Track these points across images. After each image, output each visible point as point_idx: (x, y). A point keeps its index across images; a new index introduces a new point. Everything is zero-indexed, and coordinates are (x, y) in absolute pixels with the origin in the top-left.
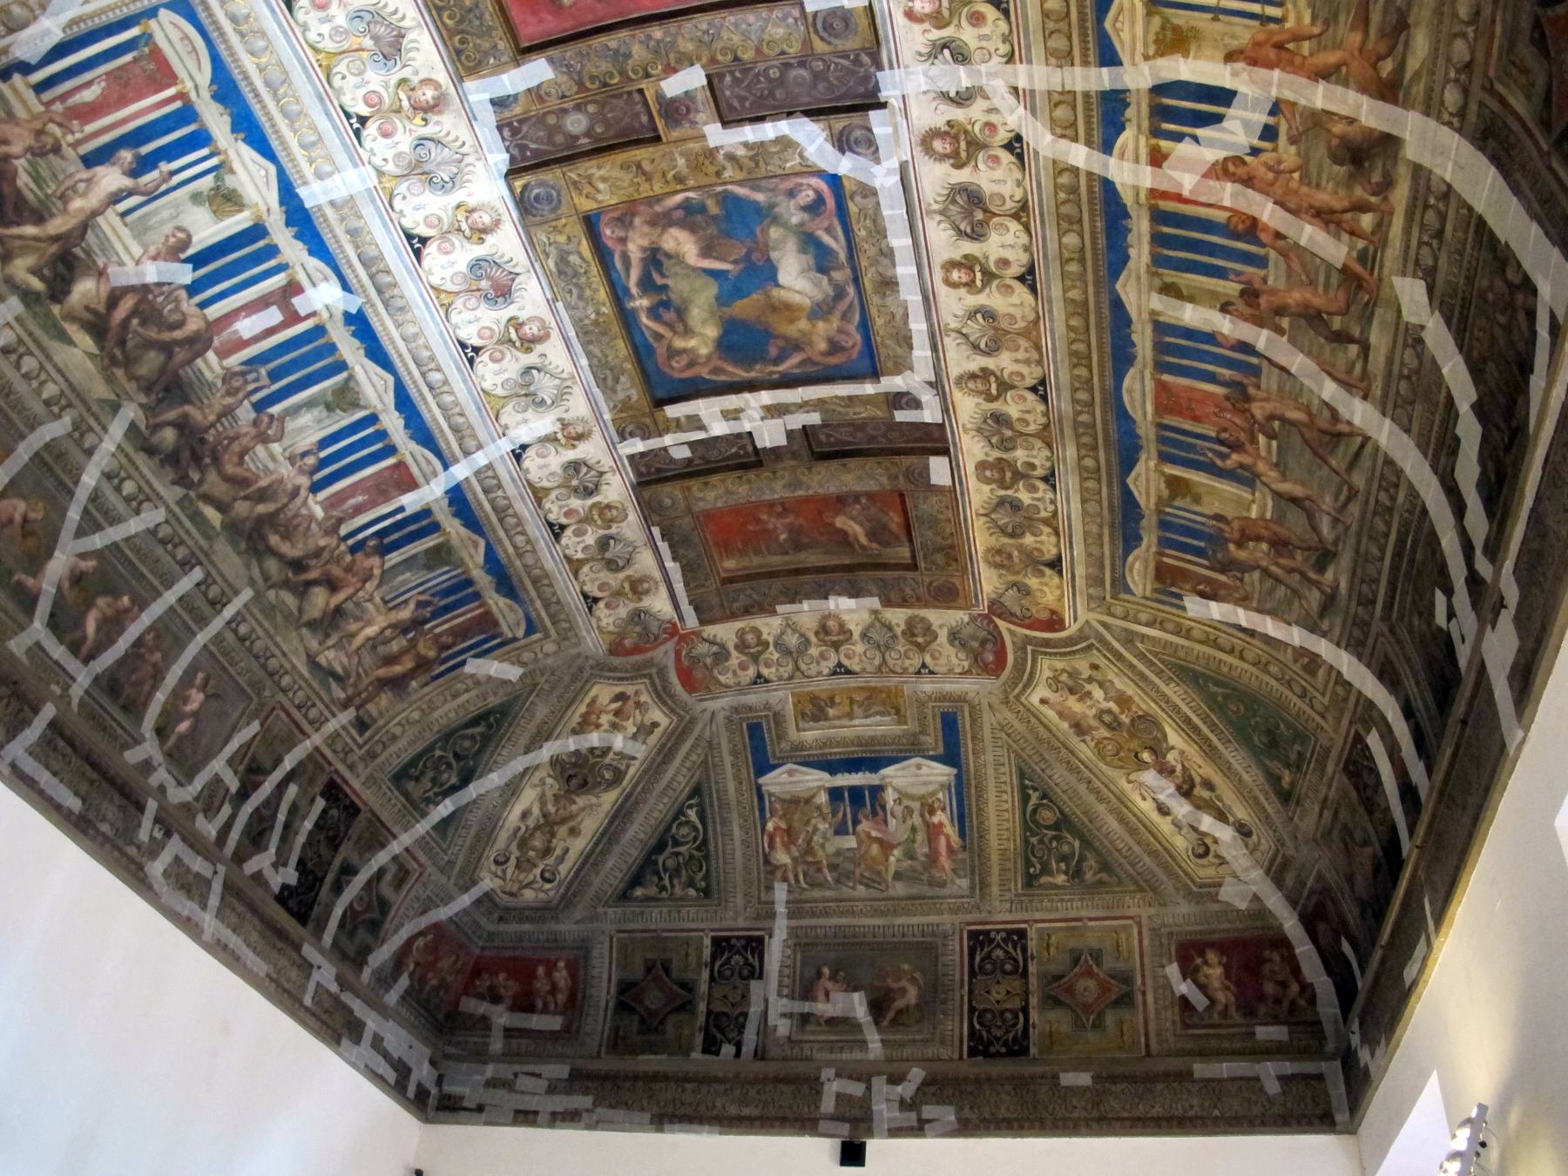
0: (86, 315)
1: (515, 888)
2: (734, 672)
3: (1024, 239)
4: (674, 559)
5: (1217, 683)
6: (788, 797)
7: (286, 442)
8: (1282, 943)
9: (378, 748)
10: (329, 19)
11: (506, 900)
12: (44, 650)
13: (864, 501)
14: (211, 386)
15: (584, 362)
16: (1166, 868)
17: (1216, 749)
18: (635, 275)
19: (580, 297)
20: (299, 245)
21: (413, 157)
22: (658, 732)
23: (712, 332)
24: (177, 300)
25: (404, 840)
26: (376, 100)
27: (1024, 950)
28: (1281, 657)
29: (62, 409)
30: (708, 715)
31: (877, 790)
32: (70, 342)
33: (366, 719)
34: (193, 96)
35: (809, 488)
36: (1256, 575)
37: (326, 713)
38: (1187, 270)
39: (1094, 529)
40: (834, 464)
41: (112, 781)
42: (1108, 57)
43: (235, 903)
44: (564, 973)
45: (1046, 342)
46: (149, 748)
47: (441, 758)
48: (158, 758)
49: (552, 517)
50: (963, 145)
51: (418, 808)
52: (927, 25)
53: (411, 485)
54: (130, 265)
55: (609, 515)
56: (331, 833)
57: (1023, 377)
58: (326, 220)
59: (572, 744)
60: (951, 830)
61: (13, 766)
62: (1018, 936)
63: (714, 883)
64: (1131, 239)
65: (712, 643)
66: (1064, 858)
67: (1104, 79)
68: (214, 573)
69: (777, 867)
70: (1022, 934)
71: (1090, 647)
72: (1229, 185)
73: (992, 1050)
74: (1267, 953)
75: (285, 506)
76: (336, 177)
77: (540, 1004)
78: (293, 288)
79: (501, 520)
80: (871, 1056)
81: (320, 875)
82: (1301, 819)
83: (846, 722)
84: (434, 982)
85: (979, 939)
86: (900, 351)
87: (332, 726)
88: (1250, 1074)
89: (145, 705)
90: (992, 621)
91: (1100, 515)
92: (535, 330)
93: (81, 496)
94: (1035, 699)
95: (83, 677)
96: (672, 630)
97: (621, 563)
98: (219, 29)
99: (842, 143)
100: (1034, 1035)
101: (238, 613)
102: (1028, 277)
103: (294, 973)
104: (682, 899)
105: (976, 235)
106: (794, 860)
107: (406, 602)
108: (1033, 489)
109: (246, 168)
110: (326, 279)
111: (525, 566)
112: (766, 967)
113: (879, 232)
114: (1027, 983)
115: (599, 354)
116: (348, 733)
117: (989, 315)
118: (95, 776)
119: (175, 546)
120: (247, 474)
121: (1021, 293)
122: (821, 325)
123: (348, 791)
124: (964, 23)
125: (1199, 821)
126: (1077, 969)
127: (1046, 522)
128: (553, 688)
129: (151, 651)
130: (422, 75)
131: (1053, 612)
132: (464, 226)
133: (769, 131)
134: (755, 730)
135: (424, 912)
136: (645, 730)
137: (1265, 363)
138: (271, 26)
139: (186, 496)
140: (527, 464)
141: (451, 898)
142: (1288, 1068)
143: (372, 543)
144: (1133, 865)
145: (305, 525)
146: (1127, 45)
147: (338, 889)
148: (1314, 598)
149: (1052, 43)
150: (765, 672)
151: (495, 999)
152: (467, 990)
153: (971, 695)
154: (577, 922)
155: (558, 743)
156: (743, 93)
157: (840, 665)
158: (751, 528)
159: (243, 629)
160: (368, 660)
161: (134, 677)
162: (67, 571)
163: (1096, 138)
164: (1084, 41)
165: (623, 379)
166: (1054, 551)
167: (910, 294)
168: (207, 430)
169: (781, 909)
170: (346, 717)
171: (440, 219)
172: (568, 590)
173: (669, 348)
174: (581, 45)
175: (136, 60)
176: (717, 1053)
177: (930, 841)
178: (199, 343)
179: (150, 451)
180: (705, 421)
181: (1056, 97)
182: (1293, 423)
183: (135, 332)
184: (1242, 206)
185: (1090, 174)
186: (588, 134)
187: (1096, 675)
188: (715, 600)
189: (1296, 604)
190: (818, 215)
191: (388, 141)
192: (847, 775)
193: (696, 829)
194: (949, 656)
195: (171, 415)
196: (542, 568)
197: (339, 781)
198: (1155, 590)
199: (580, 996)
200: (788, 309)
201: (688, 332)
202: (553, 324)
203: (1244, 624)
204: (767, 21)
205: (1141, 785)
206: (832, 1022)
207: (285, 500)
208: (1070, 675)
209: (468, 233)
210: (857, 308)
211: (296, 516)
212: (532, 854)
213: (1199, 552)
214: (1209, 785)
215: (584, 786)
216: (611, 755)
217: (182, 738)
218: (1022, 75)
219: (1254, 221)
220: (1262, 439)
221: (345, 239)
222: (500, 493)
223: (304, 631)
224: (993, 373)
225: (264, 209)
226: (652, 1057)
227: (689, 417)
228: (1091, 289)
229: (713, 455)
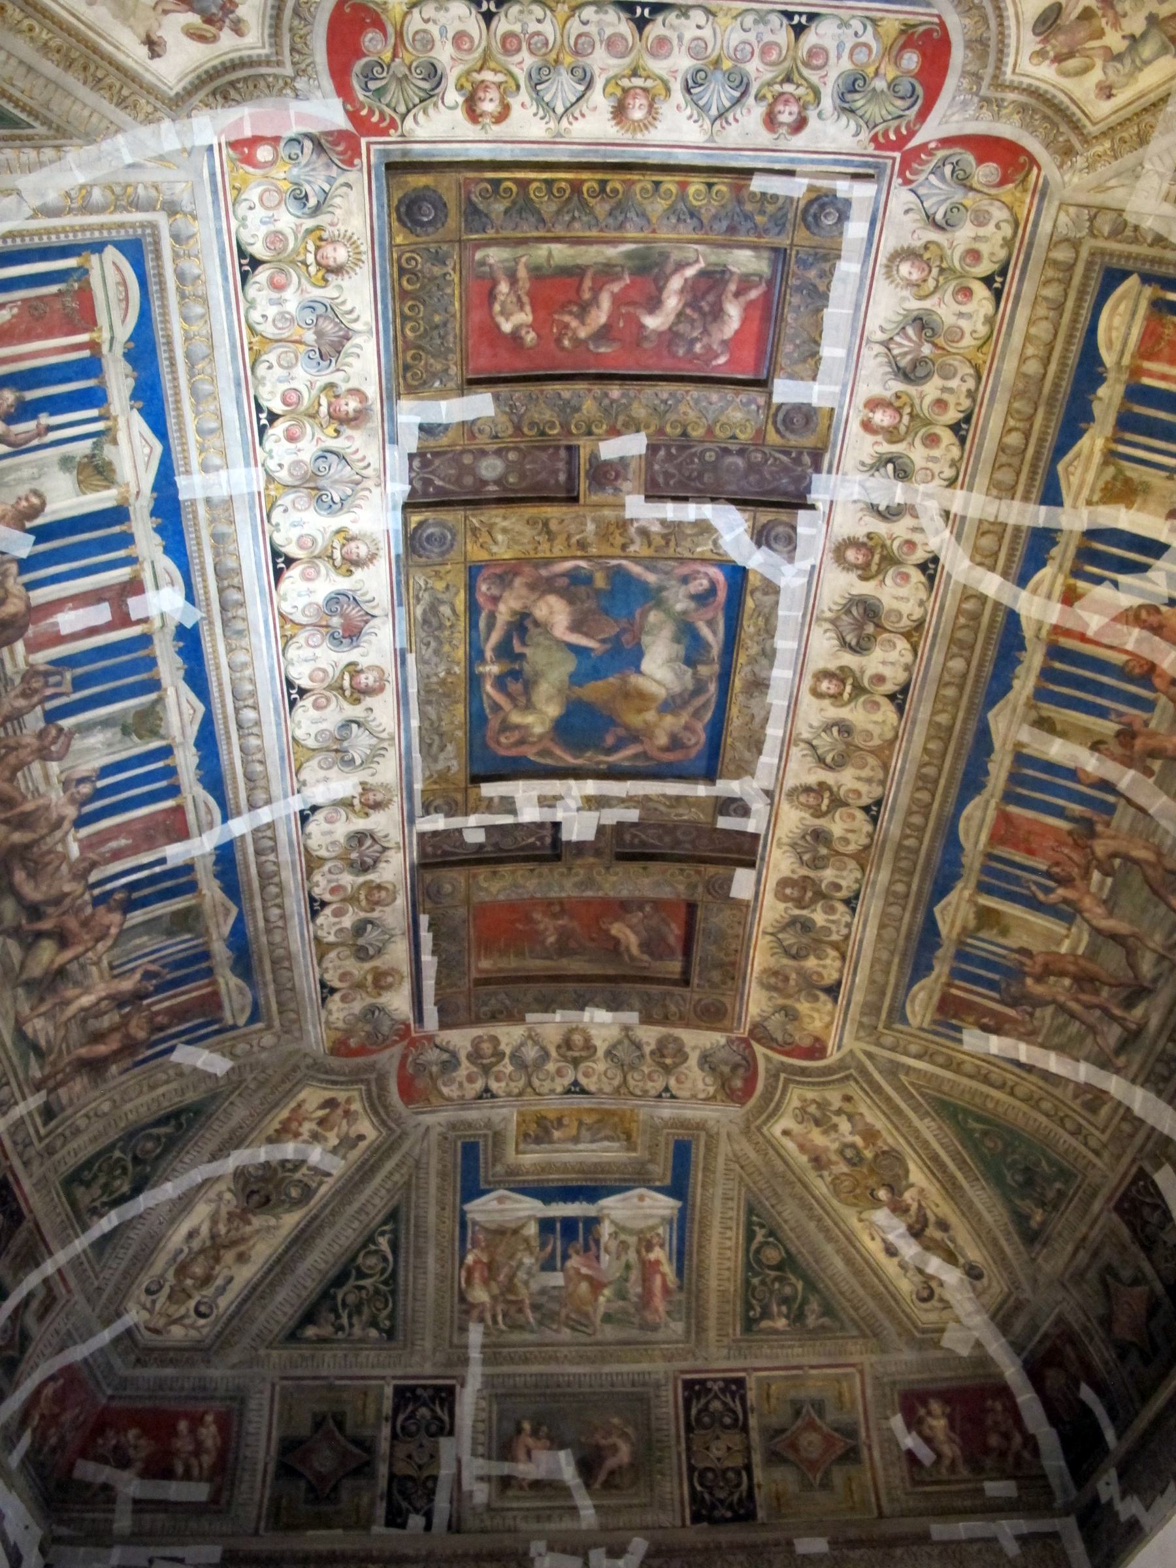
1: (160, 1323)
2: (461, 1085)
3: (908, 657)
4: (434, 953)
5: (979, 1119)
6: (493, 1226)
7: (68, 762)
8: (1003, 1391)
9: (59, 1143)
10: (280, 302)
11: (146, 1337)
13: (648, 909)
15: (415, 723)
16: (889, 1311)
17: (961, 1188)
18: (495, 637)
19: (437, 652)
20: (157, 539)
21: (311, 468)
22: (363, 1145)
23: (553, 711)
25: (61, 1257)
26: (294, 398)
28: (1058, 1092)
30: (422, 1129)
31: (592, 1223)
33: (56, 1108)
34: (105, 349)
35: (600, 888)
36: (1050, 1009)
37: (18, 1095)
38: (1075, 708)
39: (885, 956)
40: (635, 867)
42: (1052, 496)
44: (213, 1429)
45: (897, 763)
47: (119, 1160)
49: (317, 892)
50: (877, 558)
51: (81, 1218)
52: (879, 438)
53: (182, 834)
55: (376, 896)
57: (858, 794)
58: (195, 518)
59: (263, 1154)
60: (668, 1269)
62: (736, 1386)
63: (399, 1322)
64: (1020, 670)
65: (444, 1050)
66: (786, 1301)
67: (1039, 516)
69: (473, 1306)
70: (740, 1383)
71: (847, 1078)
72: (1136, 632)
73: (717, 1514)
74: (989, 1403)
75: (43, 838)
76: (223, 473)
77: (180, 1469)
78: (135, 587)
79: (263, 888)
80: (584, 1525)
82: (1046, 1260)
83: (571, 1146)
85: (694, 1389)
86: (747, 755)
87: (19, 1111)
88: (987, 1534)
90: (749, 1046)
91: (895, 941)
92: (371, 681)
94: (777, 1130)
96: (403, 1032)
97: (371, 952)
98: (162, 284)
99: (761, 537)
100: (760, 1496)
102: (899, 698)
104: (362, 1340)
105: (860, 648)
106: (494, 1298)
107: (133, 970)
108: (831, 910)
109: (131, 441)
110: (172, 584)
111: (270, 943)
112: (457, 1421)
113: (769, 631)
115: (434, 717)
117: (845, 728)
120: (16, 794)
121: (888, 712)
122: (669, 720)
124: (918, 442)
126: (799, 1422)
127: (835, 946)
128: (259, 1088)
130: (350, 385)
131: (817, 1039)
132: (337, 555)
133: (691, 512)
134: (470, 1151)
135: (61, 1350)
136: (348, 1143)
137: (1123, 802)
138: (217, 293)
140: (312, 827)
141: (92, 1334)
142: (1024, 1526)
143: (118, 896)
144: (856, 1309)
146: (1074, 488)
148: (1114, 1034)
149: (999, 476)
150: (494, 1086)
151: (123, 1463)
152: (84, 1454)
153: (711, 1123)
154: (233, 1367)
156: (672, 470)
157: (576, 1083)
158: (520, 926)
160: (75, 1034)
163: (1015, 569)
164: (1032, 478)
165: (450, 747)
166: (835, 976)
167: (777, 700)
169: (475, 1354)
170: (35, 1101)
171: (314, 541)
172: (306, 977)
173: (504, 721)
174: (533, 388)
175: (60, 293)
176: (403, 1526)
180: (518, 805)
181: (985, 527)
182: (1136, 862)
184: (1146, 653)
185: (997, 605)
186: (497, 482)
187: (848, 1107)
188: (462, 1001)
189: (1089, 1041)
190: (705, 605)
191: (292, 446)
192: (561, 1205)
193: (385, 1259)
194: (696, 1079)
196: (287, 949)
197: (11, 1179)
198: (934, 1022)
199: (231, 1456)
200: (642, 696)
201: (529, 707)
202: (392, 678)
203: (1023, 1059)
204: (730, 403)
206: (536, 1485)
207: (45, 831)
208: (820, 1106)
209: (338, 562)
210: (713, 706)
211: (50, 852)
212: (189, 1282)
213: (991, 985)
214: (943, 1226)
215: (265, 1204)
216: (304, 1170)
218: (958, 501)
219: (1152, 667)
220: (1096, 876)
221: (207, 541)
222: (272, 857)
224: (829, 789)
225: (133, 490)
226: (323, 1533)
227: (502, 798)
228: (961, 715)
229: (508, 843)
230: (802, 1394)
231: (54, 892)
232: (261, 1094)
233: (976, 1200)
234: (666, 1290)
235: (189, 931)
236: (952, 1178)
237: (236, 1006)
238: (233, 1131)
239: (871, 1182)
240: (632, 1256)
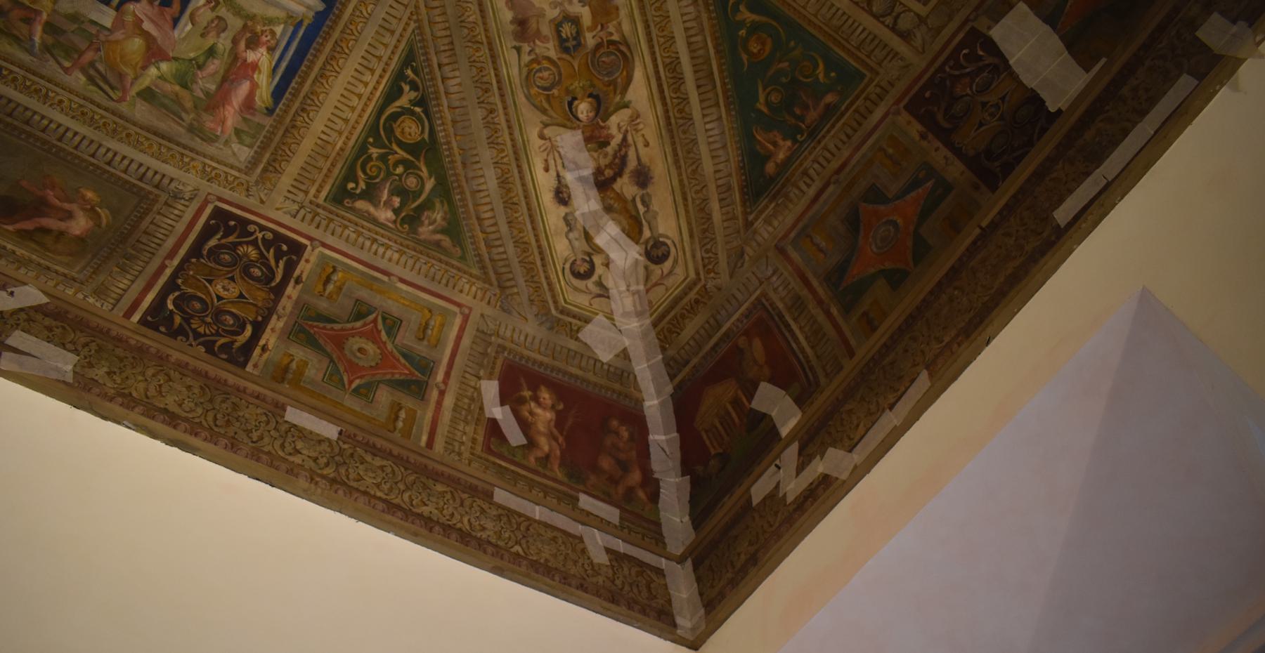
8: (638, 422)
27: (290, 267)
60: (264, 83)
66: (401, 192)
70: (297, 249)
74: (615, 423)
82: (768, 222)
114: (276, 301)
125: (599, 228)
126: (358, 324)
144: (489, 246)
177: (224, 80)
205: (554, 148)
214: (643, 178)
230: (377, 300)
233: (701, 139)
234: (248, 104)
236: (686, 100)
239: (576, 85)
240: (224, 43)
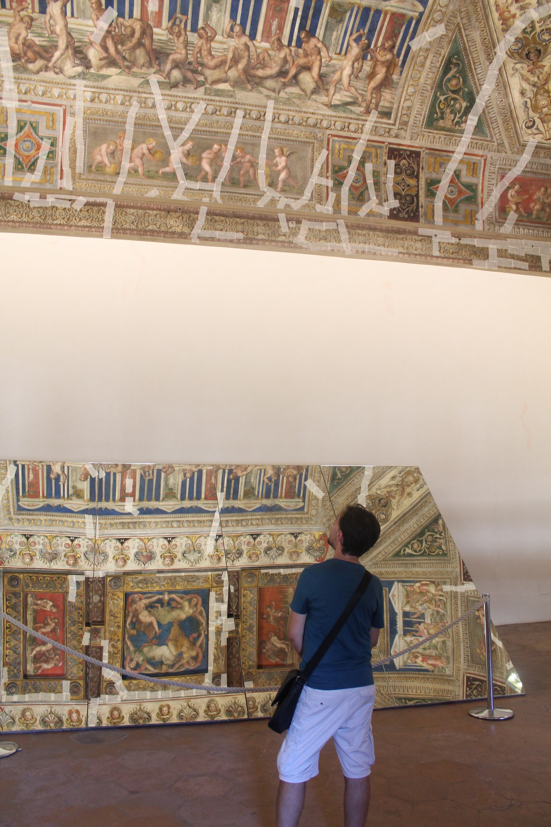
0: (103, 62)
7: (219, 32)
9: (405, 118)
12: (191, 189)
14: (169, 40)
24: (122, 24)
29: (129, 101)
32: (109, 76)
37: (360, 122)
41: (253, 218)
43: (360, 232)
46: (270, 193)
47: (446, 99)
48: (277, 195)
54: (94, 29)
56: (408, 172)
59: (510, 38)
61: (199, 238)
68: (246, 107)
75: (249, 56)
81: (414, 193)
84: (537, 207)
87: (368, 126)
89: (255, 179)
93: (165, 124)
95: (216, 188)
101: (274, 114)
103: (419, 245)
116: (381, 123)
118: (243, 220)
119: (220, 111)
120: (221, 59)
123: (405, 148)
129: (243, 157)
135: (503, 177)
139: (206, 89)
141: (516, 162)
143: (303, 35)
145: (266, 55)
147: (431, 194)
155: (502, 43)
159: (283, 119)
160: (359, 84)
161: (242, 172)
162: (181, 155)
168: (187, 57)
170: (373, 116)
178: (146, 31)
179: (175, 85)
183: (124, 50)
195: (168, 66)
197: (395, 146)
207: (246, 54)
211: (258, 56)
212: (545, 110)
217: (284, 181)
223: (314, 97)
231: (280, 62)
232: (473, 19)
235: (346, 12)
237: (410, 7)
238: (483, 43)
